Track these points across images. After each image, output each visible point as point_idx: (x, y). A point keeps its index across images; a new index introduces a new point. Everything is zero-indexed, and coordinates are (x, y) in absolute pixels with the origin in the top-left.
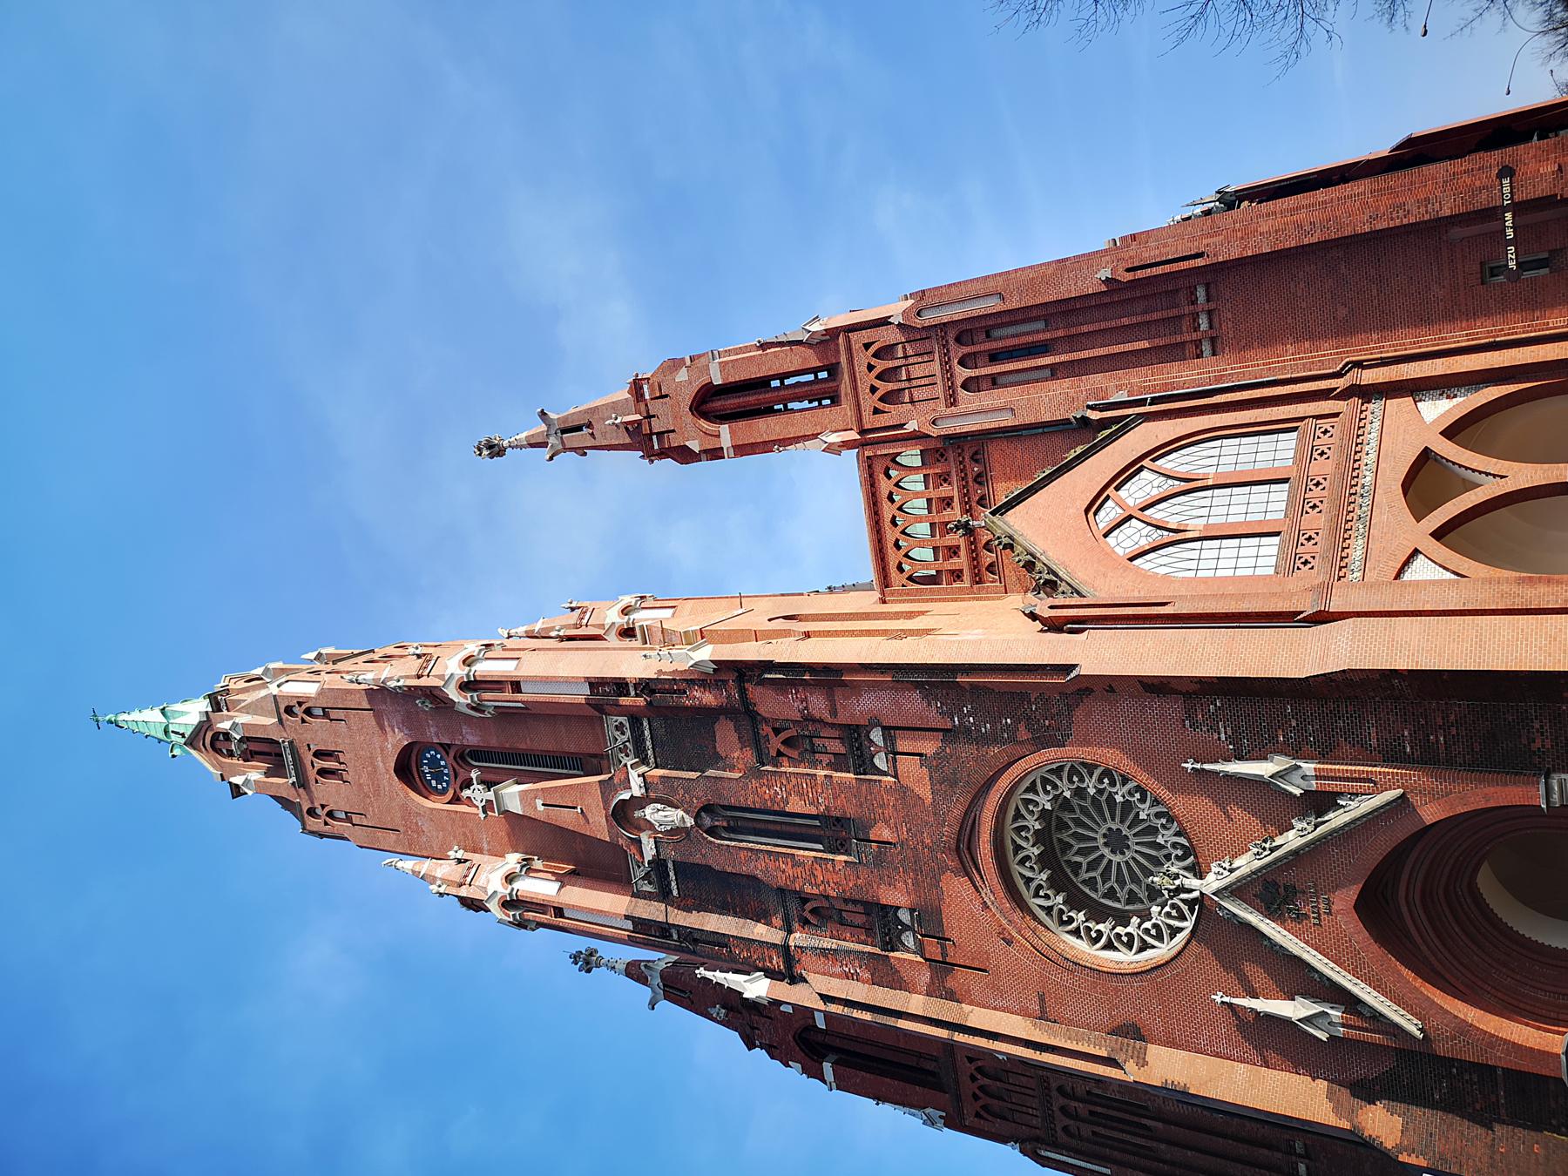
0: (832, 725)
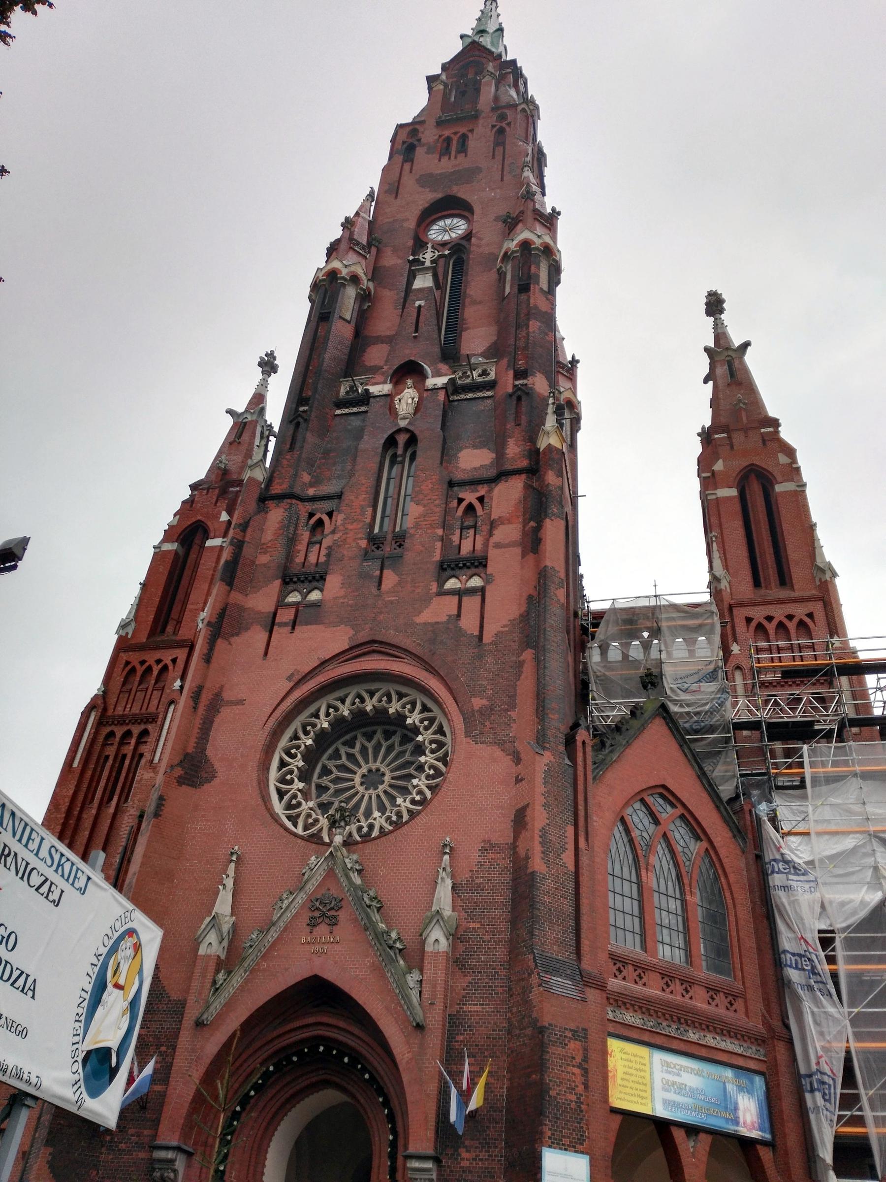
0: (486, 545)
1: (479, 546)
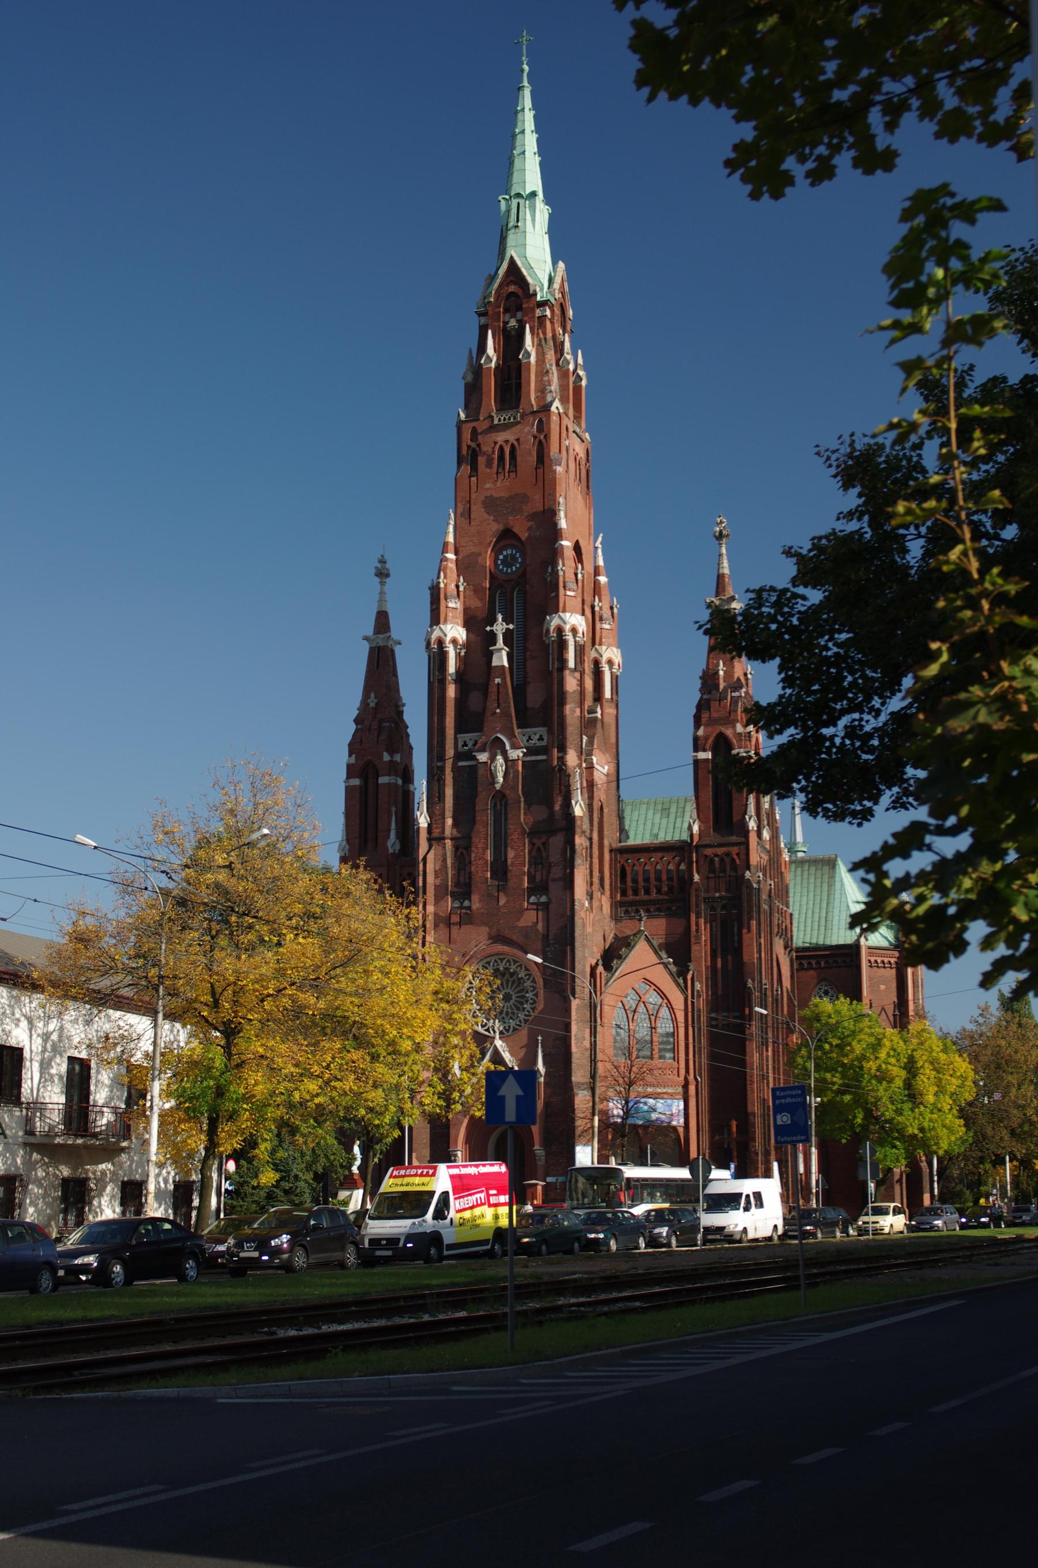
1: (544, 877)
